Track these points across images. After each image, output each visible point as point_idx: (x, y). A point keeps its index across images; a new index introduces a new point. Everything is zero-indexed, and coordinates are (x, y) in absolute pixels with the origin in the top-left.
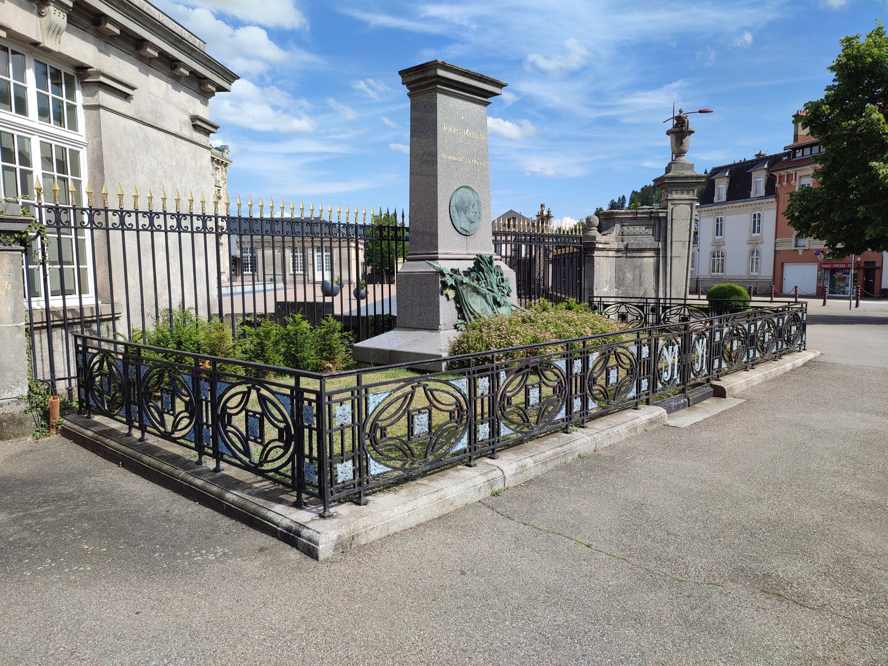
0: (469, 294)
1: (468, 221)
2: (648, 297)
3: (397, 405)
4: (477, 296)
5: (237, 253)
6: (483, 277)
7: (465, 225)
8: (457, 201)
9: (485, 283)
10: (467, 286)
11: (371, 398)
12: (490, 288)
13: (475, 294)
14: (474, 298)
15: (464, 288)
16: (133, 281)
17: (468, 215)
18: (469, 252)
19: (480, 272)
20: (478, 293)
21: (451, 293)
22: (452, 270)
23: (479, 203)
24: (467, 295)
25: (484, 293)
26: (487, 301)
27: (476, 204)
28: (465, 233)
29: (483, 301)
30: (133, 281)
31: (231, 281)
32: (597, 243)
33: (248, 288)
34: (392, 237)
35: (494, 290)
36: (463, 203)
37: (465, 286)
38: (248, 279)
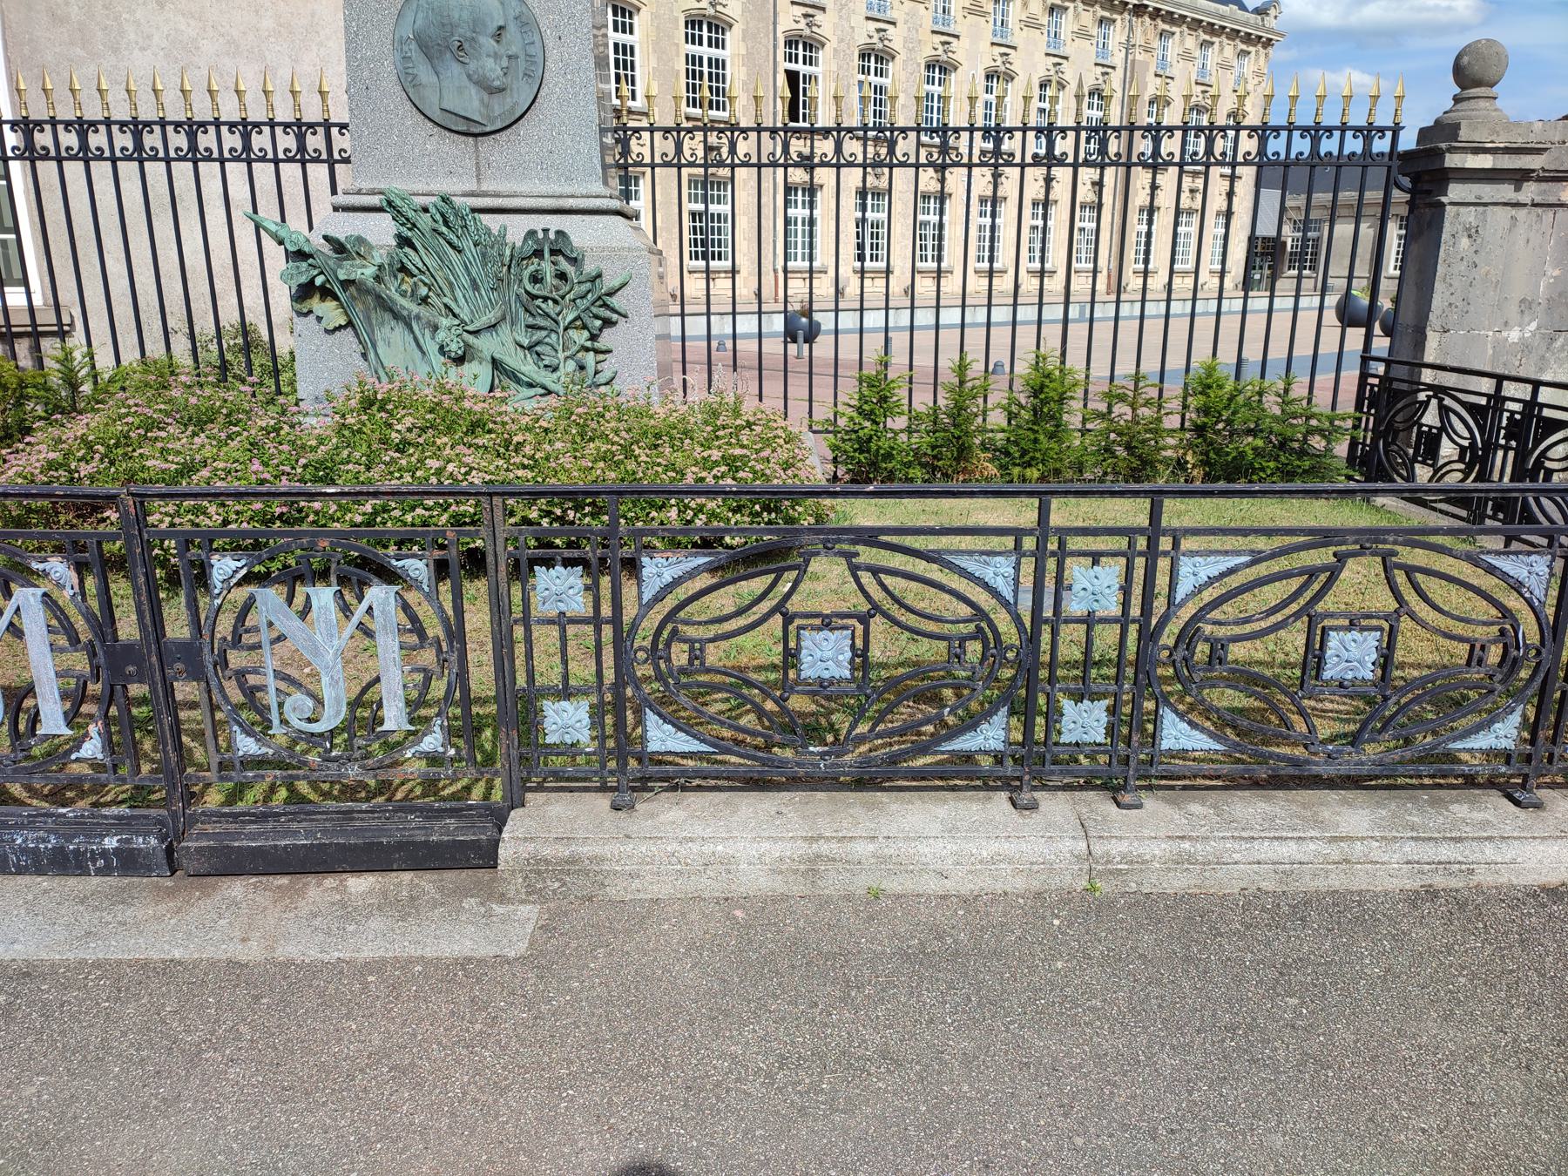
0: (373, 316)
1: (473, 90)
2: (1499, 371)
3: (1273, 594)
4: (393, 323)
5: (1267, 229)
6: (420, 265)
7: (471, 103)
8: (419, 22)
9: (425, 284)
10: (358, 290)
11: (1186, 567)
12: (446, 300)
13: (387, 316)
14: (386, 330)
15: (354, 298)
16: (116, 268)
17: (472, 66)
18: (484, 187)
19: (407, 249)
20: (396, 316)
21: (330, 312)
22: (326, 238)
23: (527, 23)
24: (369, 318)
25: (405, 313)
26: (416, 339)
27: (512, 28)
28: (463, 128)
29: (410, 339)
30: (116, 268)
31: (1247, 284)
32: (1451, 150)
33: (1283, 303)
34: (232, 150)
35: (457, 310)
36: (448, 26)
37: (352, 289)
38: (1285, 285)
